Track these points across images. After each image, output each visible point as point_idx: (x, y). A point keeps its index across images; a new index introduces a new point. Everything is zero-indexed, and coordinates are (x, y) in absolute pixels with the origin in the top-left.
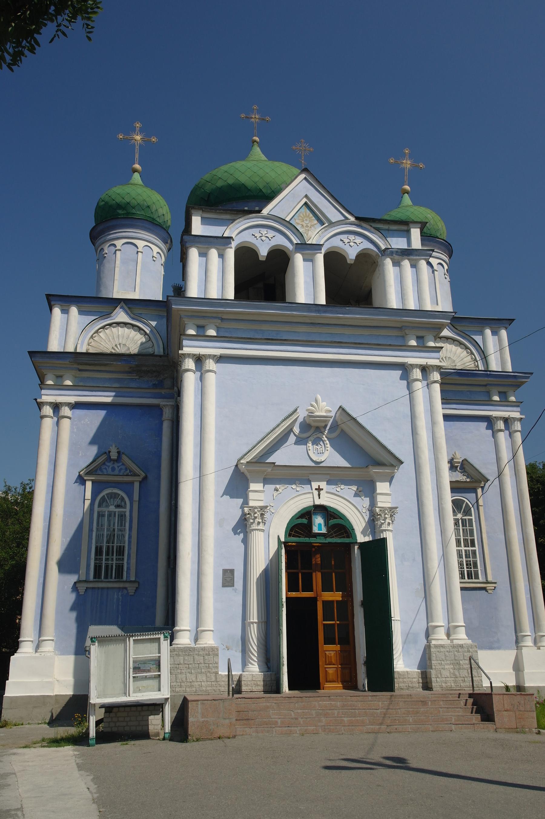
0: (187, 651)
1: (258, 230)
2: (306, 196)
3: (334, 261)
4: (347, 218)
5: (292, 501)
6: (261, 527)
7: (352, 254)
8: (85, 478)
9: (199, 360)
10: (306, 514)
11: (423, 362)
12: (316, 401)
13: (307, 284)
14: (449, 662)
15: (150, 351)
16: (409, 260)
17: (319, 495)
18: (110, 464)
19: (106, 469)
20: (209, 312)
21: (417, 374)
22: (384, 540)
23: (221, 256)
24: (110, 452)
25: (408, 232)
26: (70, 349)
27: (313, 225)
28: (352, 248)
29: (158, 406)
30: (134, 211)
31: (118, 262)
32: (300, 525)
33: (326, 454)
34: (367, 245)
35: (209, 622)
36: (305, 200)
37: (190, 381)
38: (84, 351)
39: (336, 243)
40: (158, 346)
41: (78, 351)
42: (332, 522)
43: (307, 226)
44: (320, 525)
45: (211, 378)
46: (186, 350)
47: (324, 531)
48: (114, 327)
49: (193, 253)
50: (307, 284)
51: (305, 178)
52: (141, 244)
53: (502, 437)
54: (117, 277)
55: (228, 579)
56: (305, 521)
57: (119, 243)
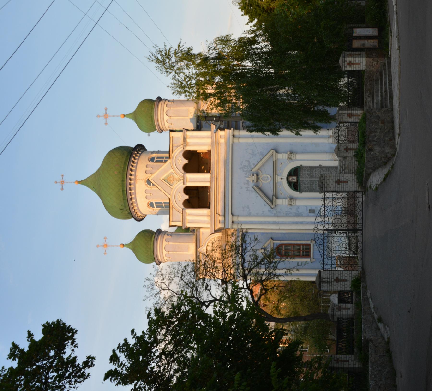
3: (187, 169)
10: (290, 183)
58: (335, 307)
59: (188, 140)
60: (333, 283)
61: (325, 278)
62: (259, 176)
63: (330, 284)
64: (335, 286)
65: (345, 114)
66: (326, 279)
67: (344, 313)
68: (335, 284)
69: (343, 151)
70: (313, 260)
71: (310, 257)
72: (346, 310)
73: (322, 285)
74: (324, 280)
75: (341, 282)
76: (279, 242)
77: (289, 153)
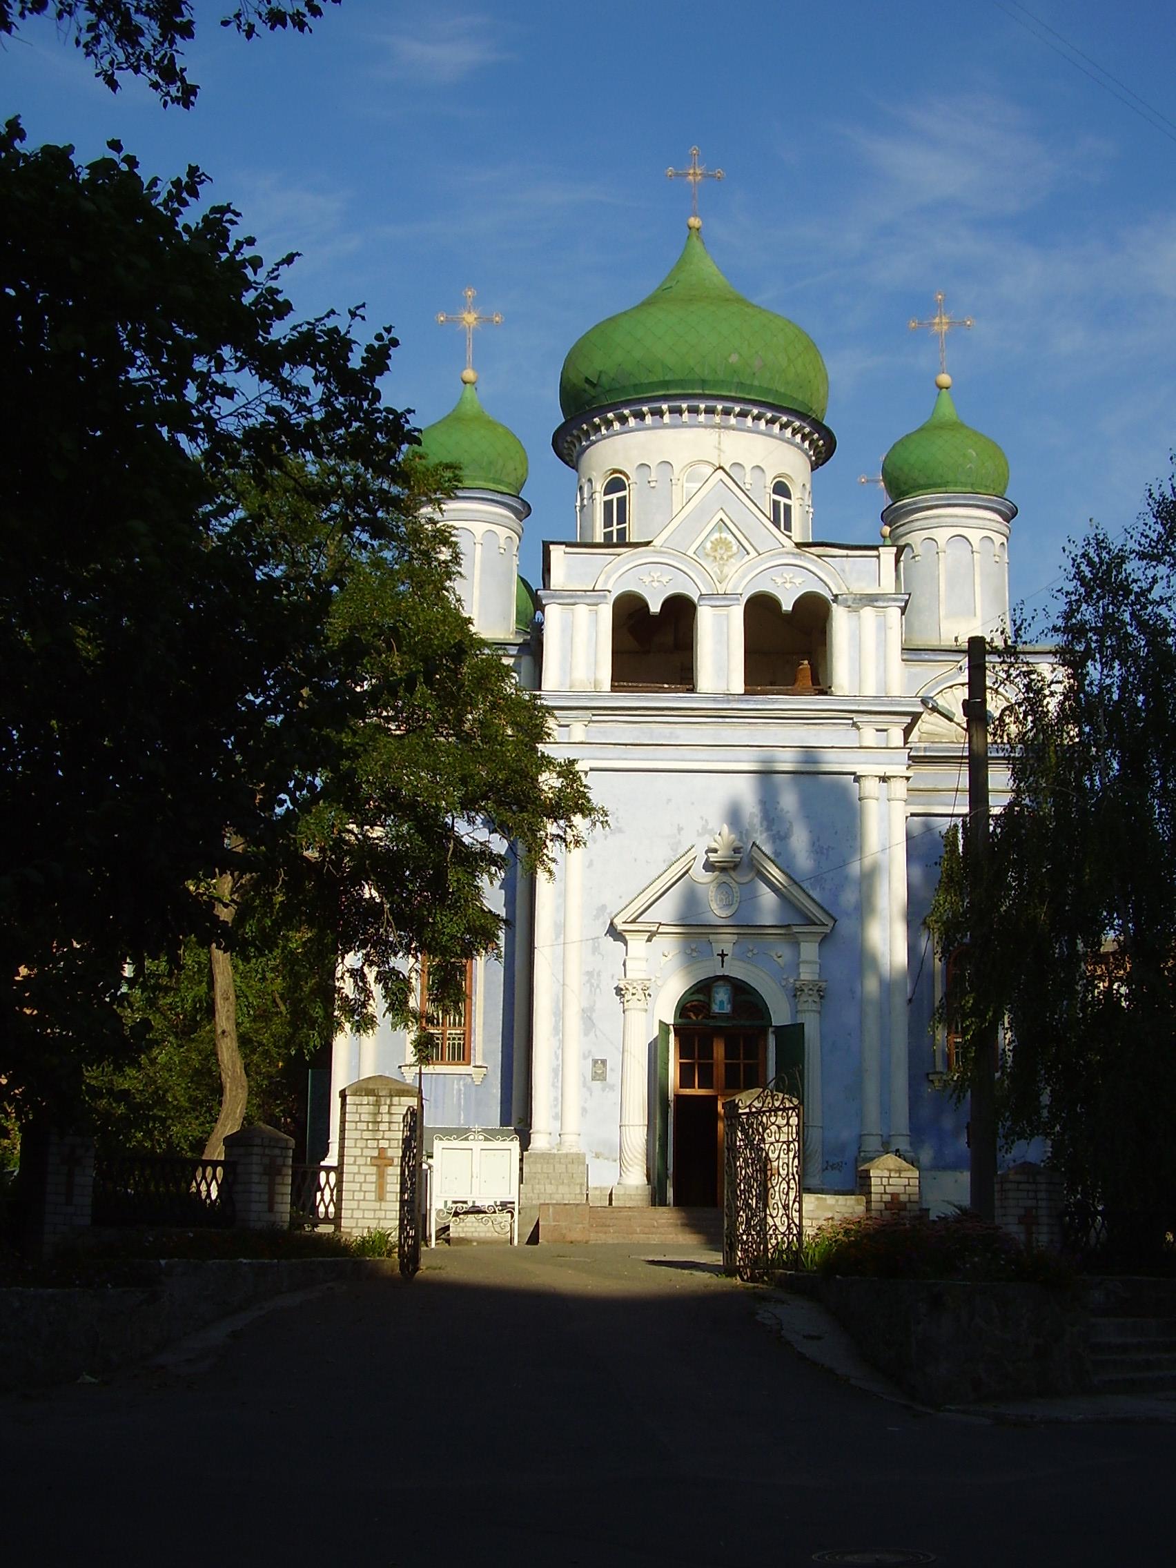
0: (546, 1157)
3: (760, 609)
11: (881, 770)
36: (721, 515)
43: (722, 558)
44: (722, 1002)
47: (727, 1009)
56: (701, 997)
58: (277, 1152)
59: (868, 612)
60: (371, 1144)
61: (389, 1113)
62: (733, 874)
63: (367, 1135)
64: (358, 1152)
65: (1036, 1198)
66: (386, 1118)
67: (255, 1188)
68: (367, 1152)
69: (889, 1189)
72: (265, 1197)
73: (365, 1100)
74: (384, 1109)
75: (374, 1178)
77: (823, 985)
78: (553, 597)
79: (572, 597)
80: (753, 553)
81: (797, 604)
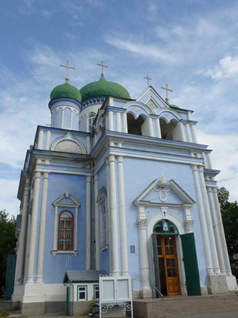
1: (135, 107)
2: (151, 96)
3: (163, 122)
4: (166, 107)
5: (155, 218)
6: (145, 228)
7: (168, 120)
8: (55, 205)
9: (116, 157)
10: (160, 223)
12: (162, 177)
13: (153, 129)
14: (217, 282)
15: (80, 153)
16: (189, 124)
17: (165, 215)
18: (65, 200)
19: (63, 201)
20: (118, 138)
21: (196, 168)
22: (192, 235)
23: (122, 115)
24: (65, 194)
25: (187, 114)
26: (48, 149)
27: (153, 108)
28: (169, 118)
29: (84, 176)
30: (69, 95)
31: (63, 115)
32: (158, 228)
33: (166, 198)
34: (175, 118)
35: (126, 268)
36: (151, 98)
37: (113, 165)
38: (53, 150)
39: (162, 115)
40: (84, 150)
41: (51, 150)
42: (170, 226)
44: (166, 227)
45: (121, 165)
46: (111, 153)
47: (167, 229)
48: (65, 141)
49: (111, 114)
50: (153, 129)
51: (150, 90)
52: (72, 109)
53: (211, 194)
54: (63, 121)
55: (132, 249)
56: (159, 226)
57: (64, 107)
59: (188, 125)
70: (54, 253)
71: (58, 250)
76: (76, 214)
78: (112, 109)
79: (116, 110)
80: (159, 108)
81: (171, 121)
